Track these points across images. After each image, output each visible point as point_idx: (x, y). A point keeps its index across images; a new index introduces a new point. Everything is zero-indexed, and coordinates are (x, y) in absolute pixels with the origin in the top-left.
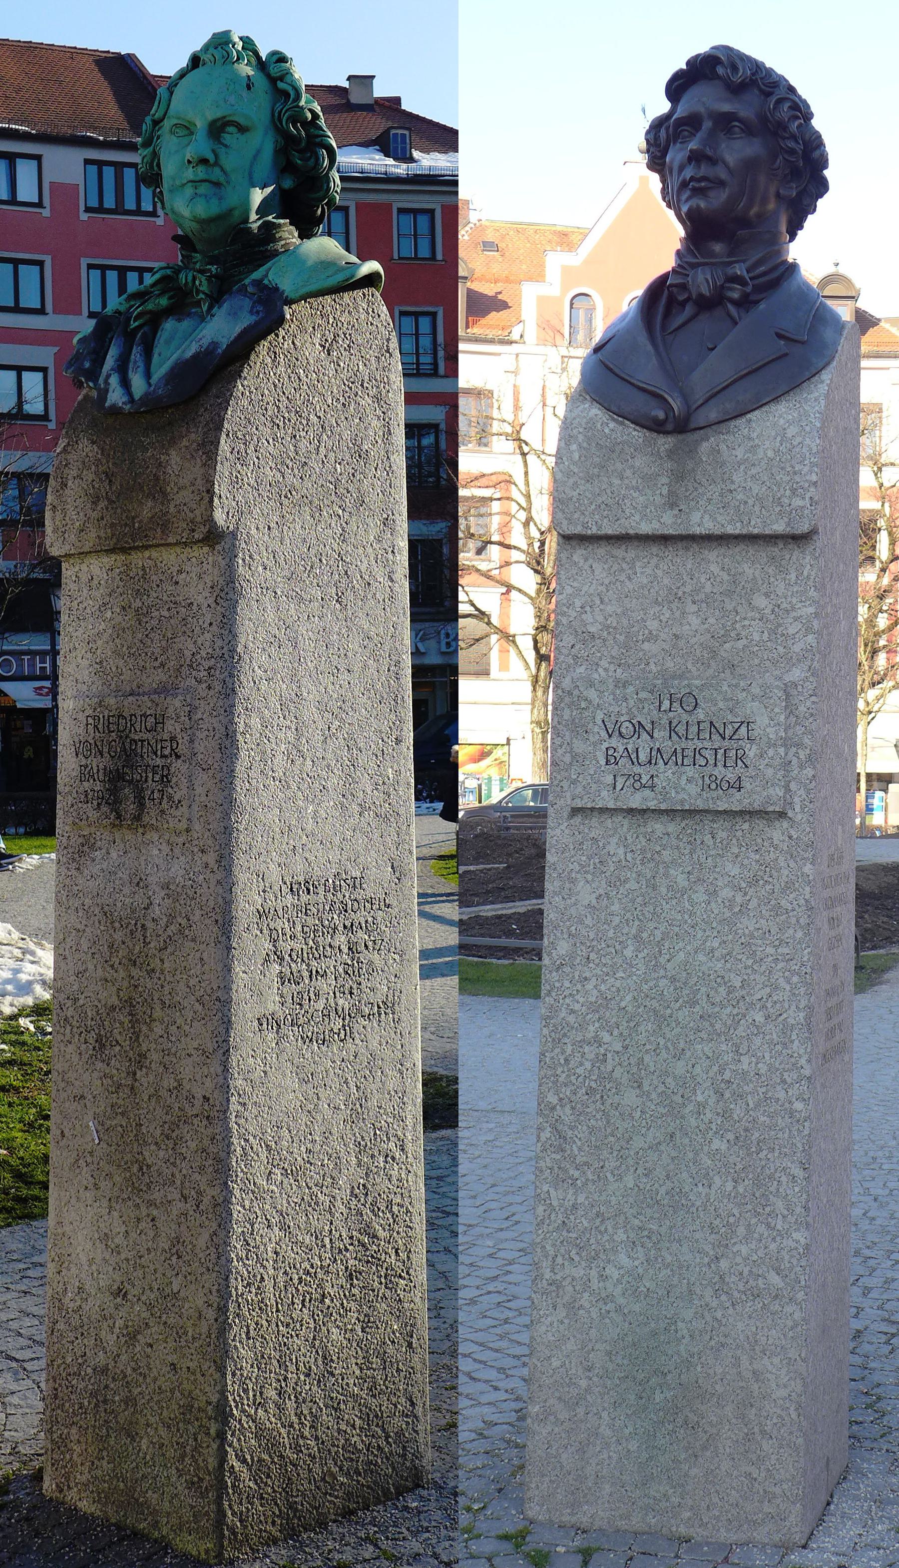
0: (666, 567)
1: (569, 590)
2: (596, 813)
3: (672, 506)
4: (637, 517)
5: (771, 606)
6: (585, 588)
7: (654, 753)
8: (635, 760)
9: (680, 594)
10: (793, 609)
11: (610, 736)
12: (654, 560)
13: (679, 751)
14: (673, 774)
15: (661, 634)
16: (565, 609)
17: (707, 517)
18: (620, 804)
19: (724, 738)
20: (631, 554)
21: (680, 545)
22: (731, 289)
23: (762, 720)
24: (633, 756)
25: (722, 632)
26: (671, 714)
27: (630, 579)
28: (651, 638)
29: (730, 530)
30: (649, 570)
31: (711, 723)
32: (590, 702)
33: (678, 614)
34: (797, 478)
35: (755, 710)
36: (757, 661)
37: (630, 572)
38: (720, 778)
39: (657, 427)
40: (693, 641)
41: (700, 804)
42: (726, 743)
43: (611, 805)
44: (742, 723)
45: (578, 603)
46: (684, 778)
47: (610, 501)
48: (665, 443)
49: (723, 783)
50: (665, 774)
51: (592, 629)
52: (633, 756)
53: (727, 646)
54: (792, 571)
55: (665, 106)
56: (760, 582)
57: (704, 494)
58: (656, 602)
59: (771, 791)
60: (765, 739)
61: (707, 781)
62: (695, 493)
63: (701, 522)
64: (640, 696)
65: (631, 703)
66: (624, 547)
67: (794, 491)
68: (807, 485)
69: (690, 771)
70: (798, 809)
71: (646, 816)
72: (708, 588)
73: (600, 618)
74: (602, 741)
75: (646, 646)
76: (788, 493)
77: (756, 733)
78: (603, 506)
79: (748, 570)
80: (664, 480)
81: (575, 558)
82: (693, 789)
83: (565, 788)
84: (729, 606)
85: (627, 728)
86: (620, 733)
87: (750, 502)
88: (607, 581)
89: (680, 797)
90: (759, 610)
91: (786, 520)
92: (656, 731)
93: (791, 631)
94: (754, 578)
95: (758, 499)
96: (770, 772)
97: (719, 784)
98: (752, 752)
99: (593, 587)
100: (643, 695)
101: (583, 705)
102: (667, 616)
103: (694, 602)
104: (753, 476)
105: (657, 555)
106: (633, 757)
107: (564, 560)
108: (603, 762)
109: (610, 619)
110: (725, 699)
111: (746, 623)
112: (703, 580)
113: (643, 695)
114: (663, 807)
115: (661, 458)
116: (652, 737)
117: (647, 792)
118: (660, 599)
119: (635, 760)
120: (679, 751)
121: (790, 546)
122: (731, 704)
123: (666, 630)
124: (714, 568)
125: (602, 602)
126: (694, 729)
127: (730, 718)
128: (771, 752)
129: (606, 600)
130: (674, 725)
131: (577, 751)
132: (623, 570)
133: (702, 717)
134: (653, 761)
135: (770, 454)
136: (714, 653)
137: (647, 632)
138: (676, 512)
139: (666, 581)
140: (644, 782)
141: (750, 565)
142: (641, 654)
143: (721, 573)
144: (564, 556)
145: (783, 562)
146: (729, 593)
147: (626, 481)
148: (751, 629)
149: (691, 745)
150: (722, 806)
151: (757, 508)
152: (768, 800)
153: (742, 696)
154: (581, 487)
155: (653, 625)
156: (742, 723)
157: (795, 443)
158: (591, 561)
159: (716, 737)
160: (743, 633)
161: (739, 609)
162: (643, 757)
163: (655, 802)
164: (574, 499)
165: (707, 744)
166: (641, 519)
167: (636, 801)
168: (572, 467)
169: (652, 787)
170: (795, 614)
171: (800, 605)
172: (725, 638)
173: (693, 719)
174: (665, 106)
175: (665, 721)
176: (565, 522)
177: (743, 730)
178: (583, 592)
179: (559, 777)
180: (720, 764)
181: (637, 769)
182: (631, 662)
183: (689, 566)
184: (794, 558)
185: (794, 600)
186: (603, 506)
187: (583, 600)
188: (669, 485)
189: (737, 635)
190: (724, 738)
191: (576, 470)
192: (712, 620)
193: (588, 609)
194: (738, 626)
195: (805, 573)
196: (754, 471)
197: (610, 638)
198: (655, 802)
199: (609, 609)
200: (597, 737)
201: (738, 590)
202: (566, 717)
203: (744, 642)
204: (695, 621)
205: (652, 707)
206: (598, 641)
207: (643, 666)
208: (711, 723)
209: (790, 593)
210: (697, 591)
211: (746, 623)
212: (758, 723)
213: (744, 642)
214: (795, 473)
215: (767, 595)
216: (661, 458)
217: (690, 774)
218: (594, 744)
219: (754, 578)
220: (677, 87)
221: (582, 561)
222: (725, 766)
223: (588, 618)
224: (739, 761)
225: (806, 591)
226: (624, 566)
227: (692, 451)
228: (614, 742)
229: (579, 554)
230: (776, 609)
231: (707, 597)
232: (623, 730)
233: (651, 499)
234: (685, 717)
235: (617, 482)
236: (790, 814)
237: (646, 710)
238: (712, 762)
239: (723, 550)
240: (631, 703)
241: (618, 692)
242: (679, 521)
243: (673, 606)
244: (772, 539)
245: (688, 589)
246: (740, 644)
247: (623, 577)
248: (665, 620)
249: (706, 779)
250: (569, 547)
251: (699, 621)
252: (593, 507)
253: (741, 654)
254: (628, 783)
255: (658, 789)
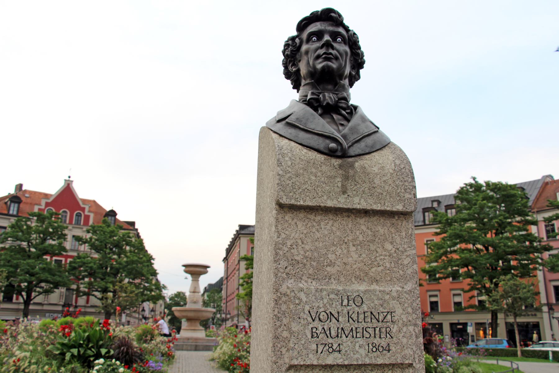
0: (337, 226)
1: (283, 236)
2: (303, 368)
3: (344, 192)
4: (325, 198)
5: (394, 249)
6: (293, 235)
7: (340, 331)
8: (329, 335)
9: (346, 241)
10: (406, 251)
11: (313, 321)
12: (331, 223)
13: (354, 329)
14: (352, 343)
15: (337, 262)
16: (281, 246)
17: (363, 200)
18: (321, 362)
19: (379, 321)
20: (318, 218)
21: (344, 214)
22: (341, 103)
23: (399, 311)
24: (328, 333)
25: (370, 262)
26: (349, 308)
27: (318, 231)
28: (331, 264)
29: (375, 207)
30: (329, 227)
31: (371, 313)
32: (301, 300)
33: (345, 251)
34: (406, 184)
35: (395, 306)
36: (389, 279)
37: (318, 227)
38: (378, 345)
39: (331, 153)
40: (354, 267)
41: (368, 361)
42: (380, 324)
43: (315, 363)
44: (388, 312)
45: (289, 243)
46: (357, 345)
47: (309, 188)
48: (336, 162)
49: (380, 348)
50: (346, 343)
51: (296, 258)
52: (328, 333)
53: (373, 270)
54: (403, 231)
55: (295, 33)
56: (388, 236)
57: (361, 188)
58: (333, 245)
59: (406, 351)
60: (401, 322)
61: (371, 347)
62: (355, 187)
63: (359, 203)
64: (330, 297)
65: (325, 301)
66: (314, 214)
67: (405, 190)
68: (411, 188)
69: (361, 341)
70: (417, 361)
71: (333, 369)
72: (361, 238)
73: (302, 252)
74: (309, 323)
75: (328, 269)
76: (403, 190)
77: (396, 318)
78: (306, 190)
79: (381, 230)
80: (339, 179)
81: (286, 218)
82: (363, 352)
83: (284, 353)
84: (372, 247)
85: (323, 316)
86: (319, 319)
87: (385, 194)
88: (305, 232)
89: (356, 356)
90: (388, 251)
91: (403, 204)
92: (340, 317)
93: (406, 262)
94: (384, 234)
95: (388, 192)
96: (405, 340)
97: (377, 348)
98: (395, 329)
99: (297, 235)
100: (332, 296)
101: (297, 302)
102: (340, 252)
103: (354, 245)
104: (384, 181)
105: (332, 219)
106: (327, 333)
107: (280, 219)
108: (309, 336)
109: (308, 253)
110: (378, 299)
111: (382, 257)
112: (358, 234)
113: (332, 296)
114: (346, 363)
115: (336, 168)
116: (338, 321)
117: (336, 354)
118: (335, 243)
119: (329, 335)
120: (354, 329)
121: (401, 219)
122: (381, 302)
123: (339, 260)
124: (363, 227)
125: (303, 243)
126: (362, 316)
127: (382, 309)
128: (405, 329)
129: (305, 242)
130: (350, 314)
131: (293, 329)
132: (313, 226)
133: (366, 309)
134: (339, 336)
135: (391, 171)
136: (367, 274)
137: (329, 261)
138: (346, 196)
139: (338, 233)
140: (334, 348)
141: (382, 228)
142: (326, 273)
143: (367, 230)
144: (280, 216)
145: (398, 226)
146: (372, 241)
147: (318, 178)
148: (385, 261)
149: (361, 325)
150: (380, 361)
151: (388, 197)
152: (404, 357)
153: (387, 297)
154: (294, 179)
155: (331, 257)
156: (388, 312)
157: (402, 167)
158: (295, 220)
159: (374, 321)
160: (381, 263)
161: (378, 249)
162: (333, 333)
163: (342, 360)
164: (290, 185)
165: (370, 325)
166: (328, 198)
167: (330, 360)
168: (288, 168)
169: (339, 351)
170: (406, 253)
171: (408, 249)
172: (371, 266)
173: (361, 311)
174: (295, 33)
175: (345, 311)
176: (285, 197)
177: (389, 317)
178: (291, 237)
179: (279, 345)
180: (377, 336)
181: (330, 340)
182: (320, 277)
183: (350, 226)
184: (403, 224)
185: (406, 246)
186: (306, 190)
187: (292, 242)
188: (342, 182)
189: (378, 264)
190: (379, 321)
191: (290, 170)
192: (364, 255)
193: (294, 246)
194: (378, 259)
195: (410, 233)
196: (385, 179)
197: (308, 264)
198: (342, 360)
199: (307, 247)
200: (306, 321)
201: (377, 240)
202: (283, 309)
203: (382, 268)
204: (355, 256)
205: (337, 303)
206: (301, 265)
207: (327, 280)
208: (371, 313)
209: (403, 243)
210: (354, 240)
211: (382, 257)
212: (397, 312)
213: (382, 268)
214: (405, 181)
215: (392, 243)
216: (336, 168)
217: (361, 343)
218: (304, 326)
219: (384, 234)
220: (302, 26)
221: (290, 220)
222: (380, 337)
223: (294, 251)
224: (388, 335)
225: (411, 242)
226: (315, 224)
227: (352, 166)
228: (317, 323)
229: (288, 217)
230: (397, 251)
231: (361, 243)
232: (321, 317)
233: (333, 188)
234: (357, 309)
235: (314, 178)
236: (414, 365)
237: (334, 305)
238: (373, 335)
239: (367, 219)
240: (325, 301)
241: (318, 295)
242: (348, 201)
243: (343, 247)
244: (391, 214)
245: (350, 238)
246: (380, 269)
247: (314, 230)
248: (338, 255)
249: (370, 345)
250: (282, 212)
251: (357, 256)
252: (301, 190)
253: (381, 274)
254: (325, 349)
255: (343, 352)
